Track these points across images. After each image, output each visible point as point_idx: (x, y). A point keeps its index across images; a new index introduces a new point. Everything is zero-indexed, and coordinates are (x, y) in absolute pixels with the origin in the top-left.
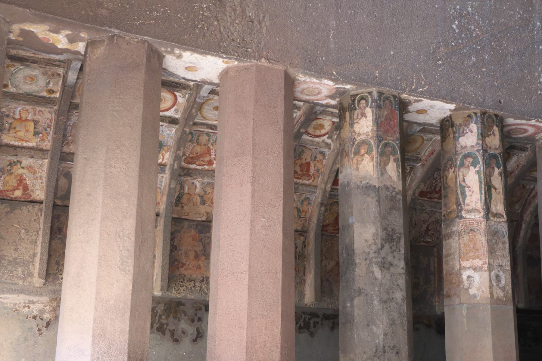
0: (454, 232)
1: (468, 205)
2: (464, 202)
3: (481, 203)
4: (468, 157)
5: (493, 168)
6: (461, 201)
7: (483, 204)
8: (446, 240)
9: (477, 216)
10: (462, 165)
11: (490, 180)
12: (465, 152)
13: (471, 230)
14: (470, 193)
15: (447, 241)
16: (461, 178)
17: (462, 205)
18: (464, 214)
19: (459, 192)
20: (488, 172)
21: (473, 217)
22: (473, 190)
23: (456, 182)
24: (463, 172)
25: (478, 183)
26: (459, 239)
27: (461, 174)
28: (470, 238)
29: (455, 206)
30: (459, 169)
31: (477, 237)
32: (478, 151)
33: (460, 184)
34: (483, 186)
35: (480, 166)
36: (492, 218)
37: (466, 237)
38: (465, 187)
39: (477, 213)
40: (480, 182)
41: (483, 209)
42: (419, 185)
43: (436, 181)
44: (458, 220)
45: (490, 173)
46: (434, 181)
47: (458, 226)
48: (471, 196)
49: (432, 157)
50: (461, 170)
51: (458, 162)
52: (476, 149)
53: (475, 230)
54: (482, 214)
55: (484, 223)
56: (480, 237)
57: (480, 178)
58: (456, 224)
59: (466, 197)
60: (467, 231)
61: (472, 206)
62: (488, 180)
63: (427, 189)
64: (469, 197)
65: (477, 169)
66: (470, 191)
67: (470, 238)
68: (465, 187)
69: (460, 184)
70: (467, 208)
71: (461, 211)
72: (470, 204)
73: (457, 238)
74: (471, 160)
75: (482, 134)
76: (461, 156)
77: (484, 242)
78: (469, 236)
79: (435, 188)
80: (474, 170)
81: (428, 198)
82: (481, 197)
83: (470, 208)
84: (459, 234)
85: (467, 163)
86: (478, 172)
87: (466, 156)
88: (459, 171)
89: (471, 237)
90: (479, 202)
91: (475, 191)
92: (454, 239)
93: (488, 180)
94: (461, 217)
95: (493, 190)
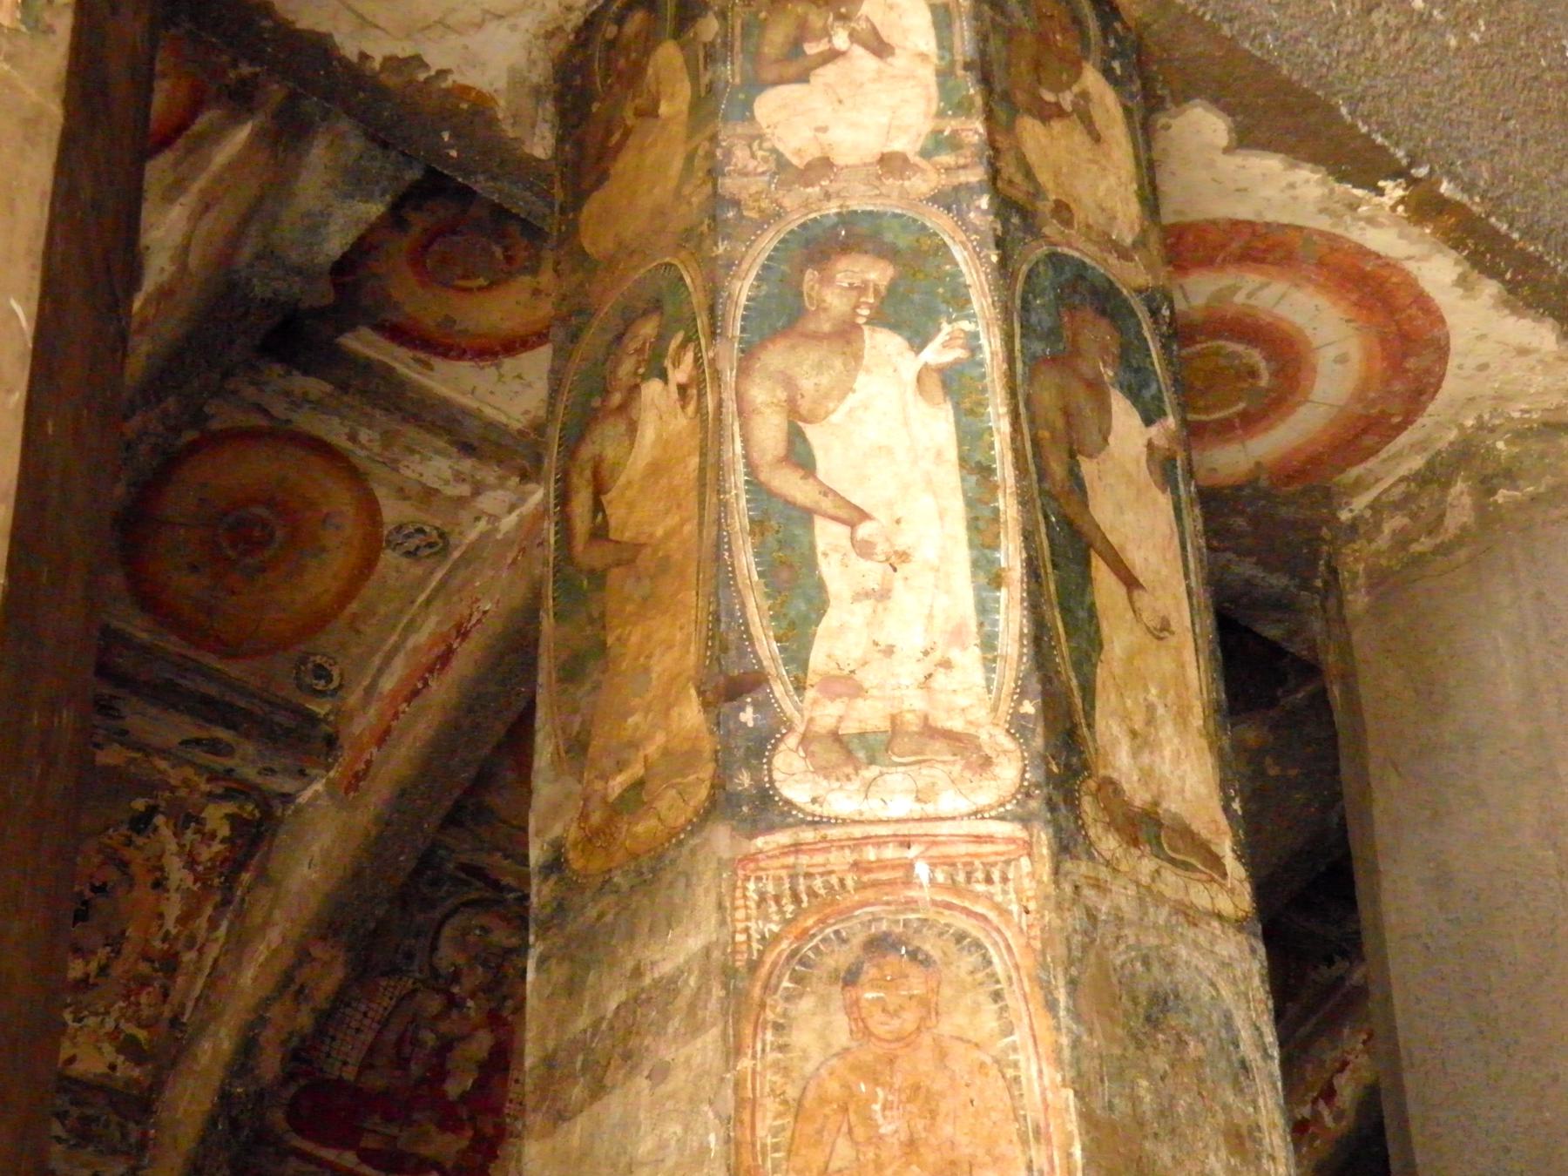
0: (670, 986)
1: (846, 685)
2: (797, 657)
3: (989, 664)
4: (846, 248)
5: (1096, 388)
6: (767, 648)
7: (1008, 675)
8: (561, 1116)
9: (949, 801)
10: (782, 315)
11: (1077, 484)
12: (804, 206)
13: (879, 945)
14: (871, 572)
15: (580, 1126)
16: (770, 432)
17: (780, 690)
18: (792, 775)
19: (746, 561)
20: (1047, 397)
21: (902, 805)
22: (901, 543)
23: (711, 476)
24: (789, 382)
25: (950, 477)
26: (734, 1051)
27: (760, 393)
28: (864, 1031)
29: (691, 715)
30: (748, 354)
31: (945, 1028)
32: (949, 200)
33: (756, 487)
34: (1008, 506)
35: (977, 331)
36: (1109, 844)
37: (817, 1031)
38: (807, 515)
39: (942, 770)
40: (977, 469)
41: (1018, 729)
42: (303, 955)
43: (452, 1002)
44: (721, 839)
45: (1067, 414)
46: (434, 1004)
47: (723, 908)
48: (882, 595)
49: (442, 691)
50: (775, 358)
51: (742, 289)
52: (923, 183)
53: (930, 947)
54: (1009, 772)
55: (1031, 873)
56: (989, 1021)
57: (970, 436)
58: (705, 902)
59: (818, 602)
60: (840, 958)
61: (893, 692)
62: (1058, 469)
63: (366, 1066)
64: (866, 607)
65: (938, 353)
66: (864, 549)
67: (867, 1033)
68: (807, 515)
69: (756, 487)
70: (827, 714)
71: (761, 746)
72: (868, 678)
73: (706, 1047)
74: (878, 273)
75: (984, 71)
76: (767, 243)
77: (1045, 1086)
78: (853, 1008)
79: (439, 1073)
80: (910, 364)
81: (366, 1157)
82: (984, 609)
83: (868, 715)
84: (739, 987)
85: (836, 302)
86: (953, 384)
87: (823, 245)
88: (743, 371)
89: (882, 1026)
90: (969, 659)
91: (926, 553)
92: (660, 1073)
93: (1058, 469)
94: (766, 808)
95: (1101, 572)
